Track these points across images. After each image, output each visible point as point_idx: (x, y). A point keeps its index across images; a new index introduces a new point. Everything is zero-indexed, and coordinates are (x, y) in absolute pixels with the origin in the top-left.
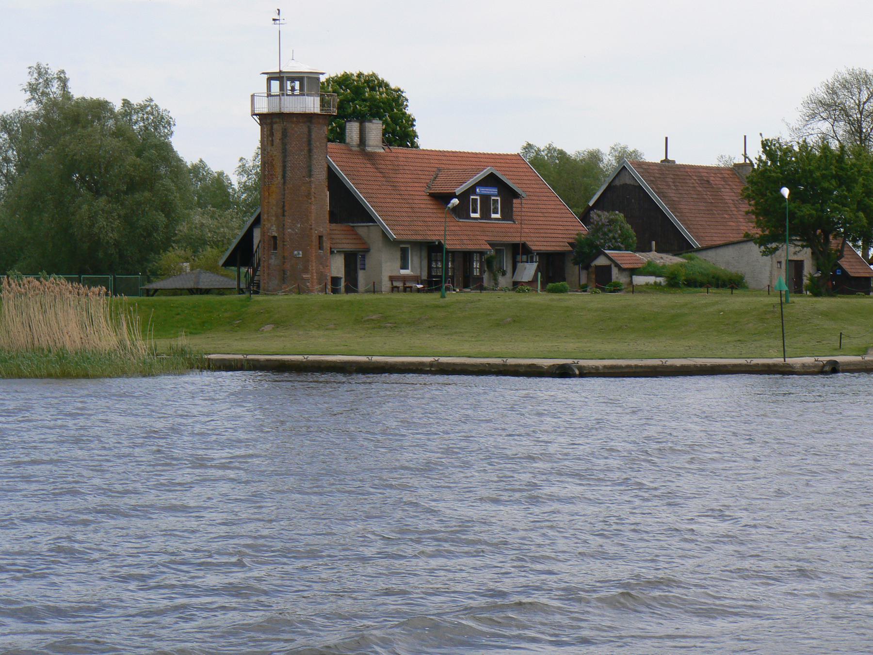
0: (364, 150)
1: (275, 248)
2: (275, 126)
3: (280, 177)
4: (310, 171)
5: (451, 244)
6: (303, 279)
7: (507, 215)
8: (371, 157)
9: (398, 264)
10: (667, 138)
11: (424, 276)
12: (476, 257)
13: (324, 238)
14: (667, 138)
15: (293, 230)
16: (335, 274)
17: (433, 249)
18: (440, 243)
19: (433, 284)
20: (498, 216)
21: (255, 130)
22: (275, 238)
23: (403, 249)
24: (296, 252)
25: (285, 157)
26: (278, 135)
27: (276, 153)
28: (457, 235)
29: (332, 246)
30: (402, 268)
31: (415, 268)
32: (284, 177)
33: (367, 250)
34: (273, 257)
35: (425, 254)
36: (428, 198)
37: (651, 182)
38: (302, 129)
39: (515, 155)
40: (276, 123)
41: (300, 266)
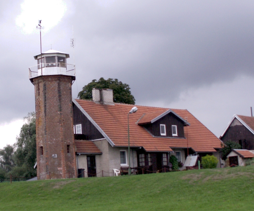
0: (102, 104)
1: (42, 154)
2: (40, 84)
3: (43, 112)
4: (60, 108)
5: (148, 148)
6: (58, 170)
7: (181, 134)
8: (106, 107)
9: (119, 161)
10: (251, 108)
11: (136, 166)
12: (165, 156)
13: (71, 146)
14: (251, 108)
15: (51, 142)
16: (80, 167)
17: (139, 151)
18: (142, 148)
19: (140, 170)
20: (176, 135)
21: (32, 87)
22: (42, 147)
23: (121, 151)
24: (53, 155)
25: (45, 100)
26: (41, 89)
27: (42, 99)
28: (151, 144)
29: (78, 151)
30: (122, 163)
31: (130, 162)
32: (45, 111)
33: (100, 154)
34: (41, 158)
35: (135, 155)
36: (138, 126)
37: (248, 124)
38: (55, 84)
39: (184, 110)
40: (40, 82)
41: (56, 163)
